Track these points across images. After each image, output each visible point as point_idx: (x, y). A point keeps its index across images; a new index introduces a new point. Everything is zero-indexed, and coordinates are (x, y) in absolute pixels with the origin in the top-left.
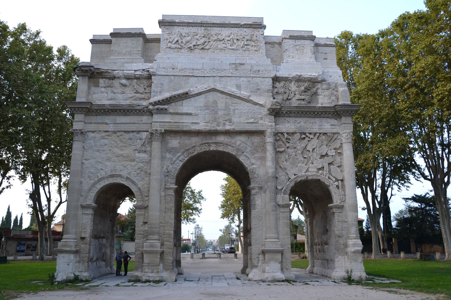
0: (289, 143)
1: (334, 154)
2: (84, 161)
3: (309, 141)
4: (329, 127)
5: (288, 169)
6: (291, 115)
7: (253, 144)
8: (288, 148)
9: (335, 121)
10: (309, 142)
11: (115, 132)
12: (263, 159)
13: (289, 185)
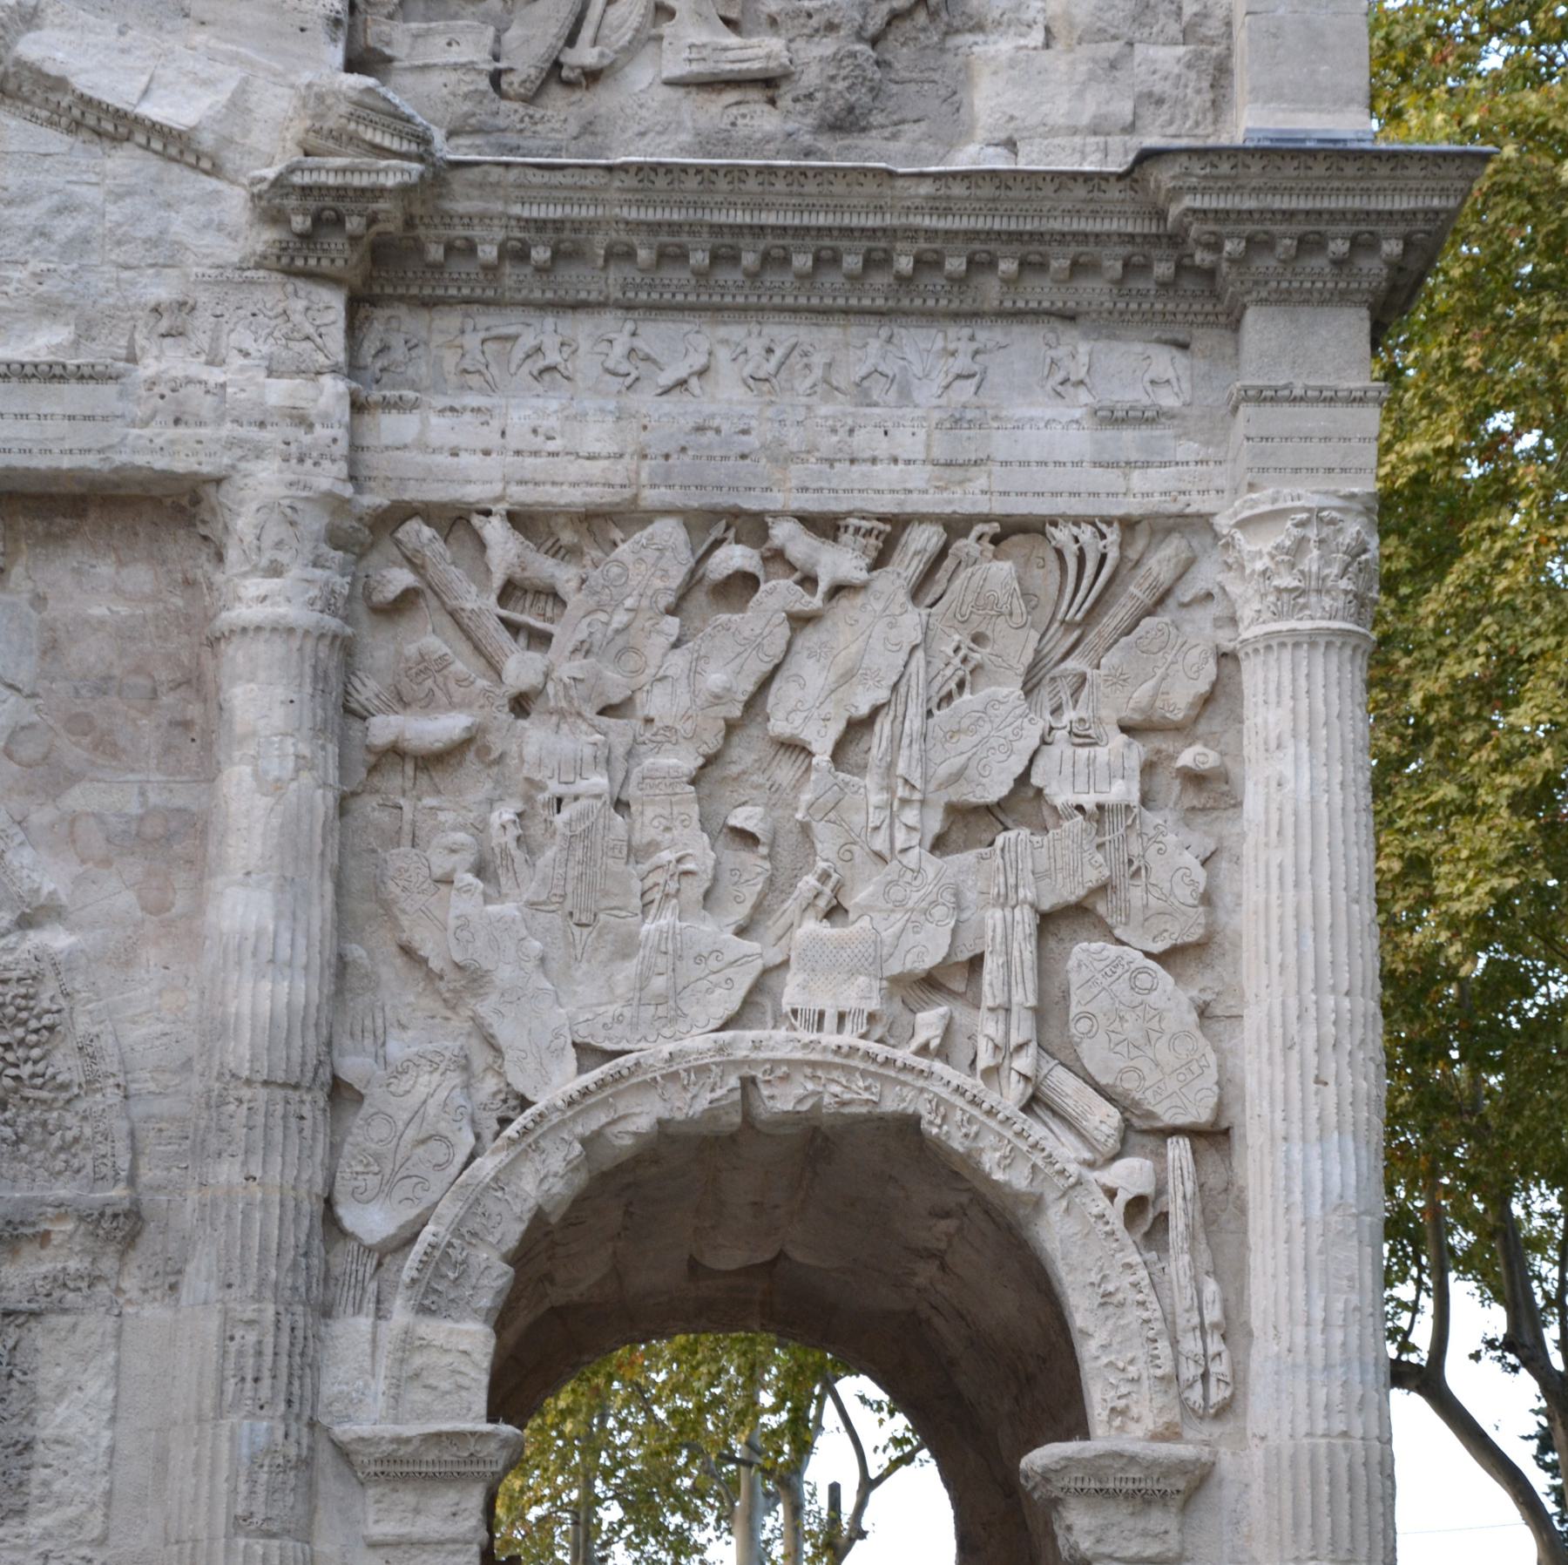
0: (541, 639)
1: (1123, 791)
3: (800, 621)
4: (1080, 441)
5: (504, 974)
6: (577, 280)
7: (51, 648)
8: (521, 705)
9: (1164, 362)
10: (810, 638)
12: (177, 844)
13: (498, 1181)
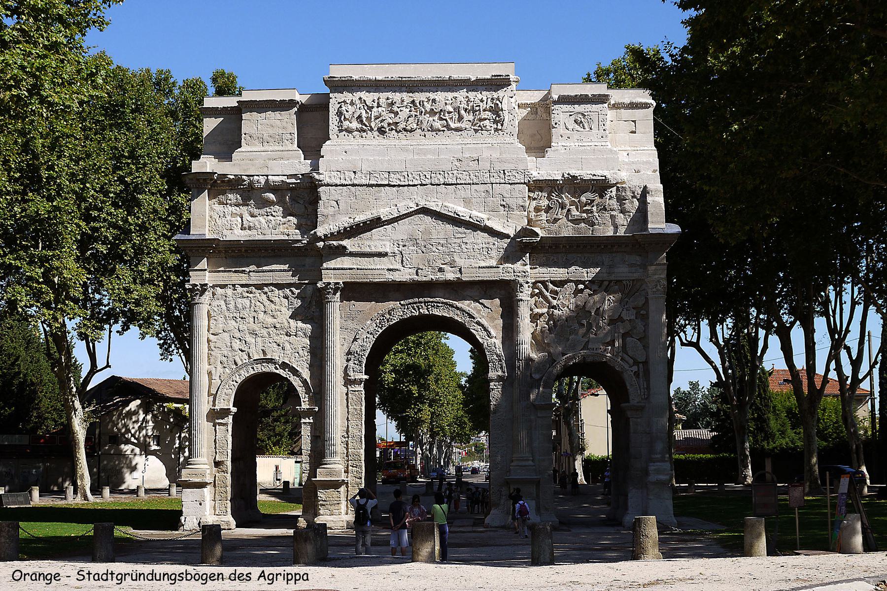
0: (555, 299)
1: (633, 317)
2: (212, 337)
9: (638, 258)
11: (259, 287)
